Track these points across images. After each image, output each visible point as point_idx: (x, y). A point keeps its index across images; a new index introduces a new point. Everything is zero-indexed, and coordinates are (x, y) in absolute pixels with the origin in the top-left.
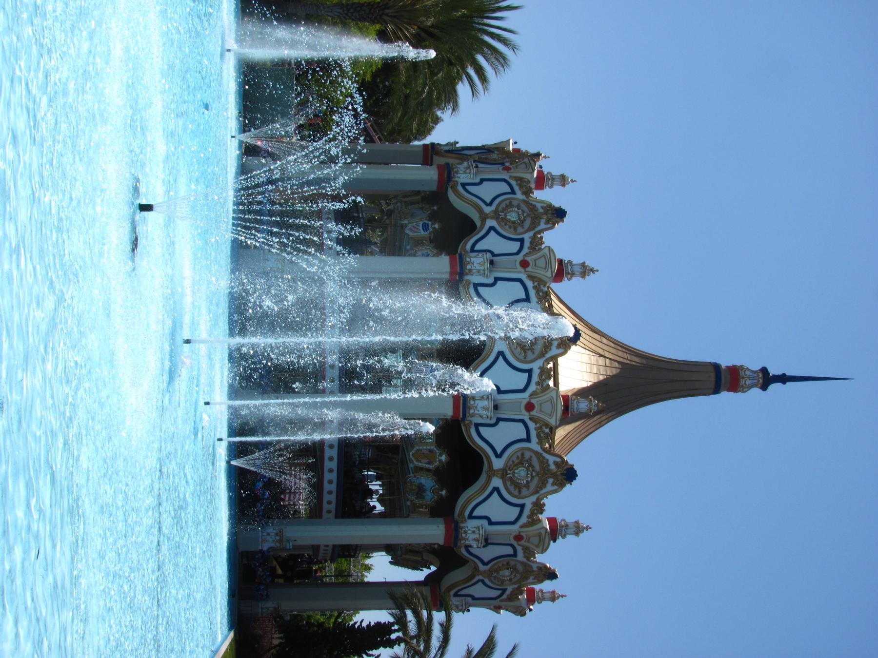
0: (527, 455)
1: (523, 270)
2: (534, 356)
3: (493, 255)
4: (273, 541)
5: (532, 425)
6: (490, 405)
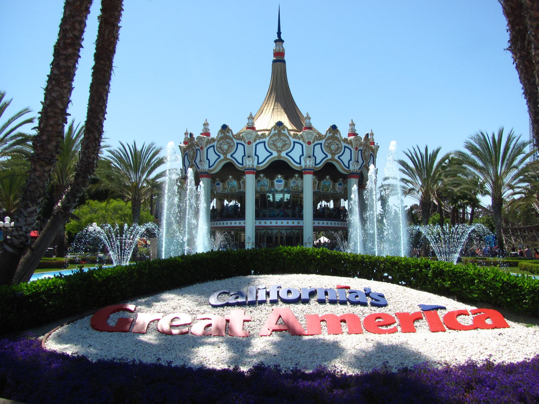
0: (326, 144)
1: (252, 144)
2: (288, 141)
3: (245, 155)
5: (316, 142)
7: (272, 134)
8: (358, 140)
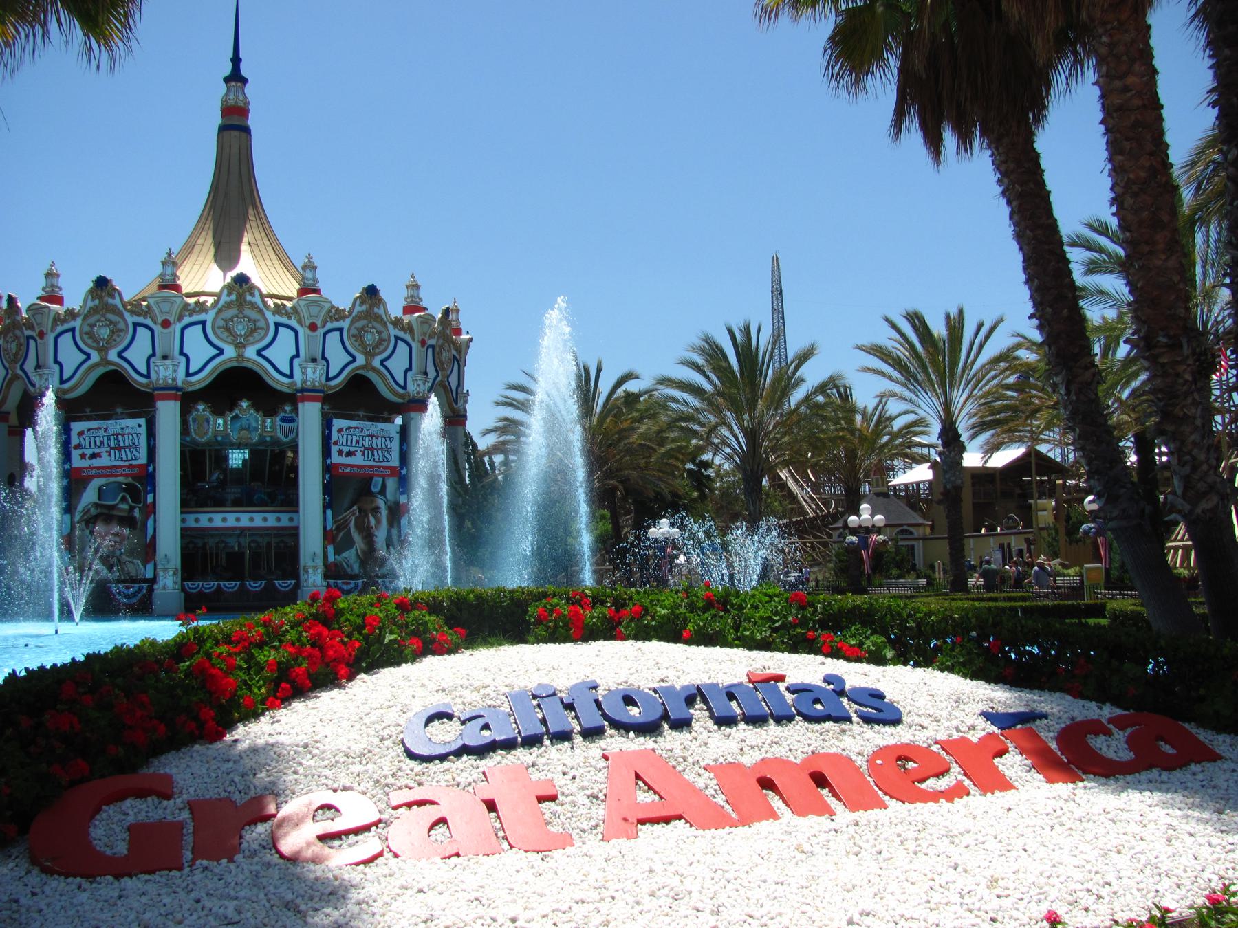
0: (354, 331)
3: (154, 354)
5: (329, 326)
7: (222, 302)
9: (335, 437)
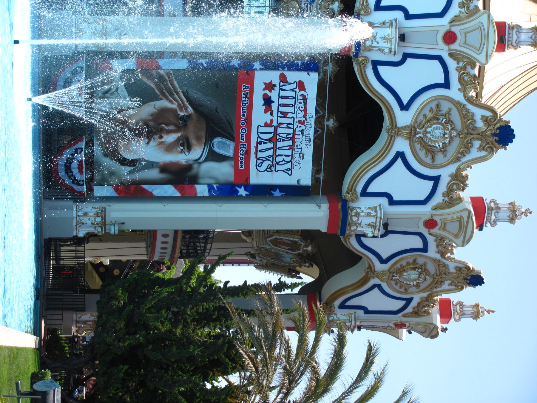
0: (445, 106)
4: (92, 224)
5: (452, 64)
6: (394, 34)
8: (460, 228)
9: (293, 76)
